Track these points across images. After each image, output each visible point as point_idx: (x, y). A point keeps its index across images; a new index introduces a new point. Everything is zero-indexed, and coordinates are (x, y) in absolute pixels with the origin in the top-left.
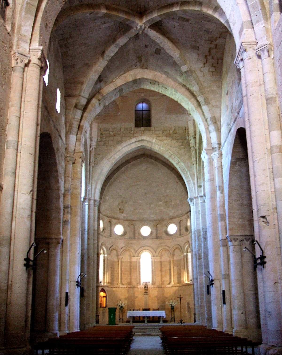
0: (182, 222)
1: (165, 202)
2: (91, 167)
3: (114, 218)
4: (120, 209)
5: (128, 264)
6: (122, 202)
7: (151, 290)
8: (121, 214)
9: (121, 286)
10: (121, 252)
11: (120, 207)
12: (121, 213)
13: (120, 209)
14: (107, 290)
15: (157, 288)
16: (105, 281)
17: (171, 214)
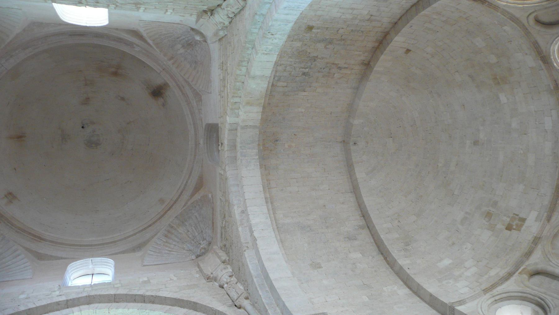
0: (546, 19)
1: (499, 83)
2: (246, 304)
3: (528, 254)
4: (507, 229)
6: (489, 215)
8: (524, 228)
11: (500, 226)
12: (521, 226)
13: (509, 228)
17: (531, 61)
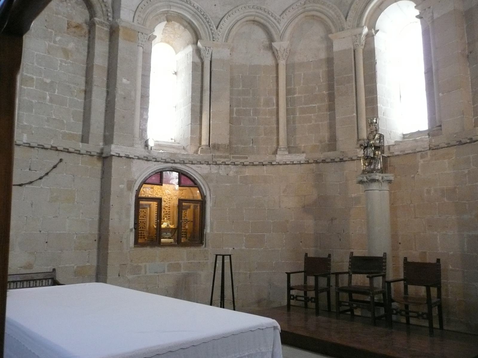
5: (322, 71)
7: (421, 161)
9: (282, 156)
10: (281, 27)
14: (205, 177)
15: (453, 150)
16: (204, 142)
